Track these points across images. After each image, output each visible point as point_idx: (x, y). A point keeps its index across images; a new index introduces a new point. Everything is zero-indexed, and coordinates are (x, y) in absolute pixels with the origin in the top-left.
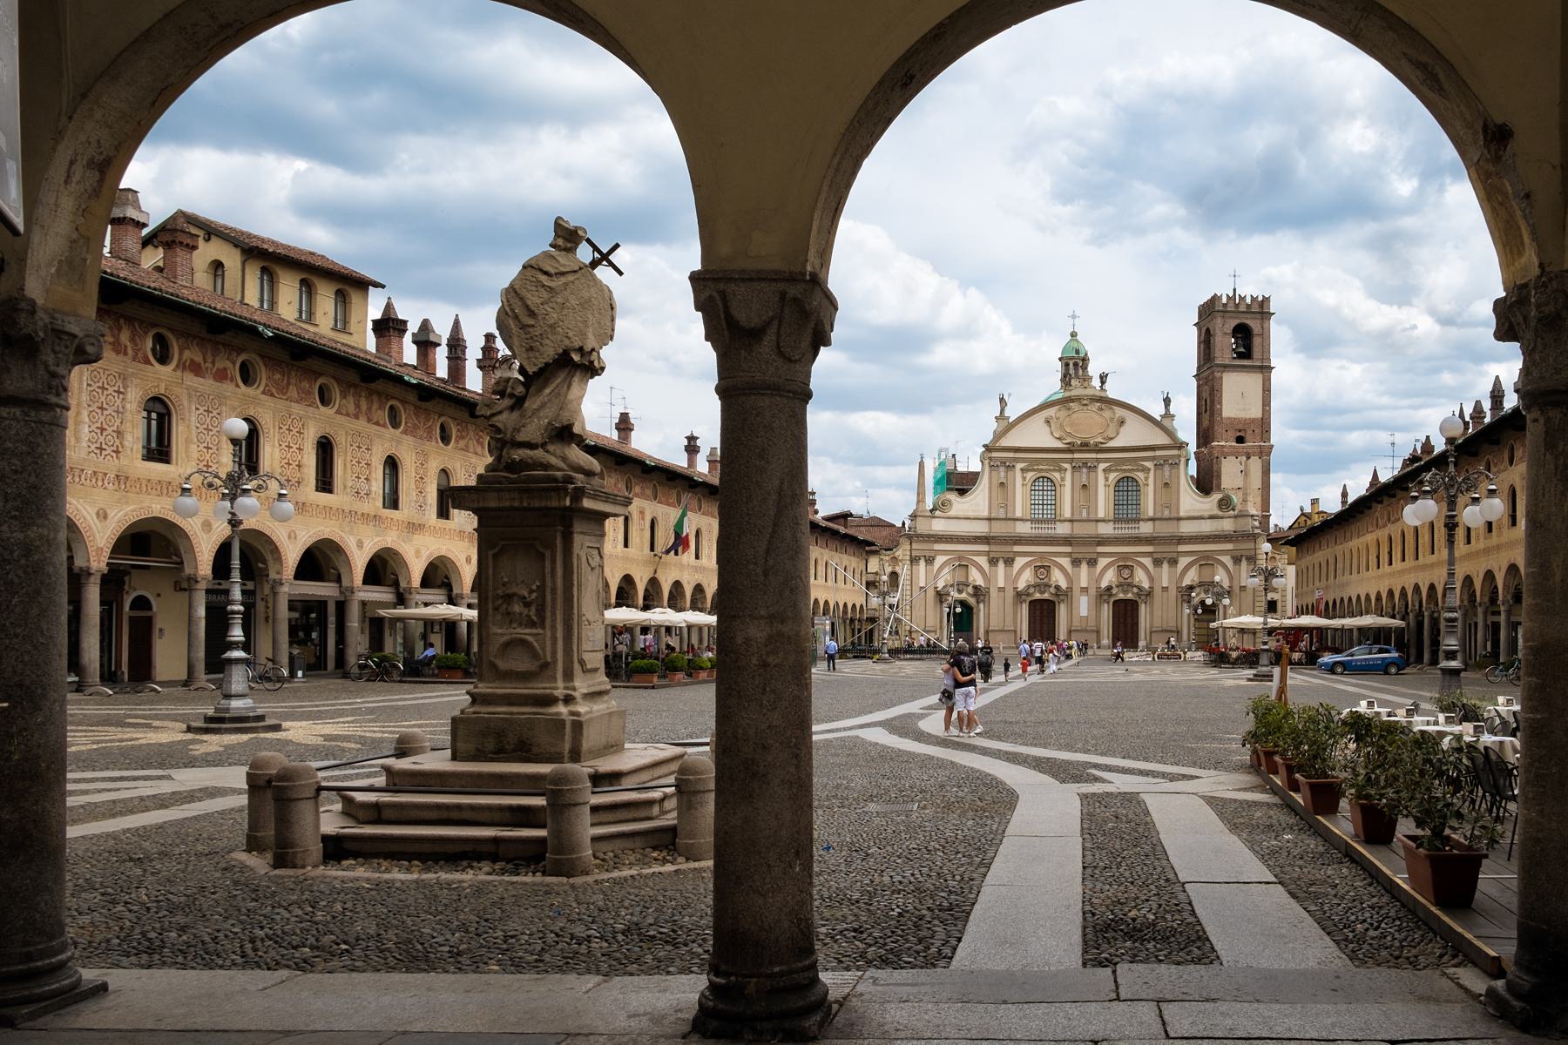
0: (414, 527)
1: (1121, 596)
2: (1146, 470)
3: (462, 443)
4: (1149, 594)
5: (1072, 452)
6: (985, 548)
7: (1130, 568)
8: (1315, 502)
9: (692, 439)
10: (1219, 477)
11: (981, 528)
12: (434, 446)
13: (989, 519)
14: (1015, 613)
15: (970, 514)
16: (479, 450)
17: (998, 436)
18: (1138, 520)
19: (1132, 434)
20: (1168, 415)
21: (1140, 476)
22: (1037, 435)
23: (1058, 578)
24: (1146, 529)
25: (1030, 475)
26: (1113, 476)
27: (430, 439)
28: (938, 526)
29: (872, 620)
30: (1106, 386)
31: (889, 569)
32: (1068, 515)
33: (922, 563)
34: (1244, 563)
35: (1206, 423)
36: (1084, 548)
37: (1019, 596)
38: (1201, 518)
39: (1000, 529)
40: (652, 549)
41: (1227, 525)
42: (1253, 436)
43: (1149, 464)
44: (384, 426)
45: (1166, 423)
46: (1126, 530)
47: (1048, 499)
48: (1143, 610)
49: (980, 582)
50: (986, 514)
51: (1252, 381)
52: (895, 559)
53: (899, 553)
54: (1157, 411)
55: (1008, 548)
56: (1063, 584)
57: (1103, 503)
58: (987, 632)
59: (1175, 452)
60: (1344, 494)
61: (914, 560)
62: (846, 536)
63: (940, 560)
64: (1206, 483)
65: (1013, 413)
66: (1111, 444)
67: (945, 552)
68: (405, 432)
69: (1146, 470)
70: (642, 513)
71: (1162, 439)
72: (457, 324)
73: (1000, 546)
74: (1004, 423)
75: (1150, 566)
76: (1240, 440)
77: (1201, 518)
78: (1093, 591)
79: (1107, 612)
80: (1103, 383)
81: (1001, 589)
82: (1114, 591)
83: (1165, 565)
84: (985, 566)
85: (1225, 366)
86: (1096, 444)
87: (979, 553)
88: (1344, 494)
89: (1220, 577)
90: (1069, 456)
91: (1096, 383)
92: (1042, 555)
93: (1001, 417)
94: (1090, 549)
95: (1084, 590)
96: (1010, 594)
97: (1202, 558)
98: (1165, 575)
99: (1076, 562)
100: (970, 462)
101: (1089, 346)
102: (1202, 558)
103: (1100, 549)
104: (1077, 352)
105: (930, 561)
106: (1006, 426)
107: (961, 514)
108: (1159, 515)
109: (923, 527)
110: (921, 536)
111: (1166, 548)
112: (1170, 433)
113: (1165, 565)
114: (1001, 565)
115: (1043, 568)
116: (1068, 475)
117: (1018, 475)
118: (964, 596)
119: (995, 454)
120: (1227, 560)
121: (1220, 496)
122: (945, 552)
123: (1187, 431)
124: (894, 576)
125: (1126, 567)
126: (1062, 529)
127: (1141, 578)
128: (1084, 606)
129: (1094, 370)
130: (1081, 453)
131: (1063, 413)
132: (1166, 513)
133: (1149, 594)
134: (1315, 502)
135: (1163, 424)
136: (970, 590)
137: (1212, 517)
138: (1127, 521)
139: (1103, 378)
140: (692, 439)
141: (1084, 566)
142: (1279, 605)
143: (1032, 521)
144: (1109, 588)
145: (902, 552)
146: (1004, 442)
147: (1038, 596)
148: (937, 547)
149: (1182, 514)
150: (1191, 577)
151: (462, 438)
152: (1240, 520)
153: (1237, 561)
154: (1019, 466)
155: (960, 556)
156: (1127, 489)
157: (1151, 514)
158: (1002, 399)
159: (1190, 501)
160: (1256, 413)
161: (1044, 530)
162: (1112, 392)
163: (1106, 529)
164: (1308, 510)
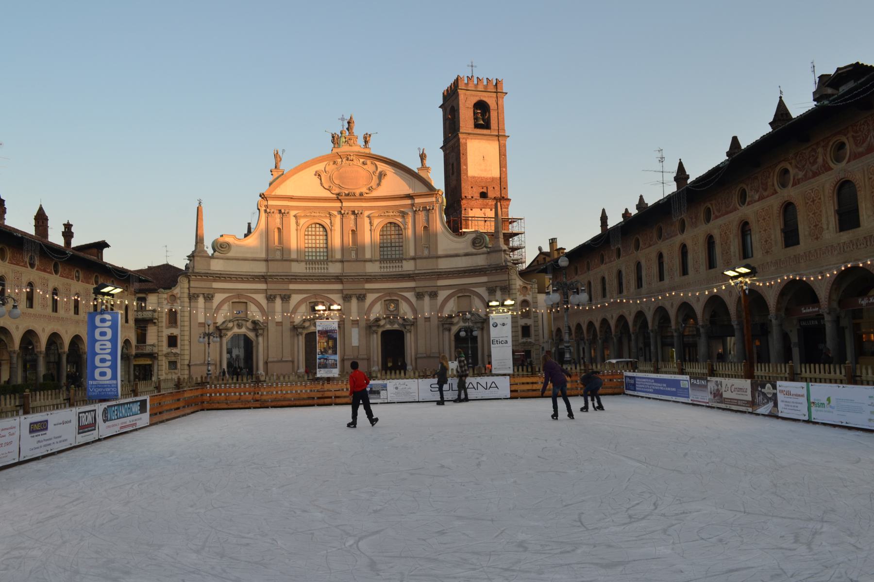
1: (388, 327)
6: (263, 286)
7: (396, 302)
8: (553, 242)
11: (260, 268)
13: (267, 260)
14: (293, 345)
18: (401, 260)
20: (424, 167)
24: (408, 267)
28: (217, 266)
30: (370, 145)
33: (201, 300)
38: (457, 256)
39: (276, 268)
41: (480, 261)
45: (422, 174)
46: (391, 269)
48: (409, 339)
49: (259, 317)
50: (263, 256)
52: (173, 298)
53: (176, 291)
54: (414, 165)
58: (266, 363)
60: (604, 219)
61: (192, 297)
63: (218, 298)
66: (374, 194)
67: (224, 291)
76: (484, 195)
77: (457, 256)
78: (363, 324)
79: (376, 340)
80: (366, 142)
82: (382, 323)
83: (427, 299)
84: (263, 302)
86: (361, 194)
87: (257, 291)
88: (604, 219)
91: (361, 142)
94: (359, 286)
95: (355, 323)
97: (460, 291)
98: (427, 308)
101: (354, 119)
102: (460, 291)
103: (368, 286)
105: (209, 298)
107: (238, 255)
109: (200, 267)
111: (428, 283)
113: (427, 299)
116: (337, 220)
117: (293, 221)
118: (243, 330)
119: (271, 203)
122: (224, 291)
125: (392, 301)
128: (355, 337)
129: (359, 131)
132: (426, 253)
133: (414, 323)
134: (553, 242)
137: (466, 255)
138: (391, 260)
141: (354, 301)
142: (532, 330)
143: (306, 262)
144: (377, 320)
146: (280, 191)
148: (216, 285)
149: (440, 252)
150: (450, 308)
152: (494, 255)
154: (293, 213)
155: (239, 294)
157: (412, 253)
158: (276, 155)
160: (496, 174)
161: (318, 270)
164: (546, 249)
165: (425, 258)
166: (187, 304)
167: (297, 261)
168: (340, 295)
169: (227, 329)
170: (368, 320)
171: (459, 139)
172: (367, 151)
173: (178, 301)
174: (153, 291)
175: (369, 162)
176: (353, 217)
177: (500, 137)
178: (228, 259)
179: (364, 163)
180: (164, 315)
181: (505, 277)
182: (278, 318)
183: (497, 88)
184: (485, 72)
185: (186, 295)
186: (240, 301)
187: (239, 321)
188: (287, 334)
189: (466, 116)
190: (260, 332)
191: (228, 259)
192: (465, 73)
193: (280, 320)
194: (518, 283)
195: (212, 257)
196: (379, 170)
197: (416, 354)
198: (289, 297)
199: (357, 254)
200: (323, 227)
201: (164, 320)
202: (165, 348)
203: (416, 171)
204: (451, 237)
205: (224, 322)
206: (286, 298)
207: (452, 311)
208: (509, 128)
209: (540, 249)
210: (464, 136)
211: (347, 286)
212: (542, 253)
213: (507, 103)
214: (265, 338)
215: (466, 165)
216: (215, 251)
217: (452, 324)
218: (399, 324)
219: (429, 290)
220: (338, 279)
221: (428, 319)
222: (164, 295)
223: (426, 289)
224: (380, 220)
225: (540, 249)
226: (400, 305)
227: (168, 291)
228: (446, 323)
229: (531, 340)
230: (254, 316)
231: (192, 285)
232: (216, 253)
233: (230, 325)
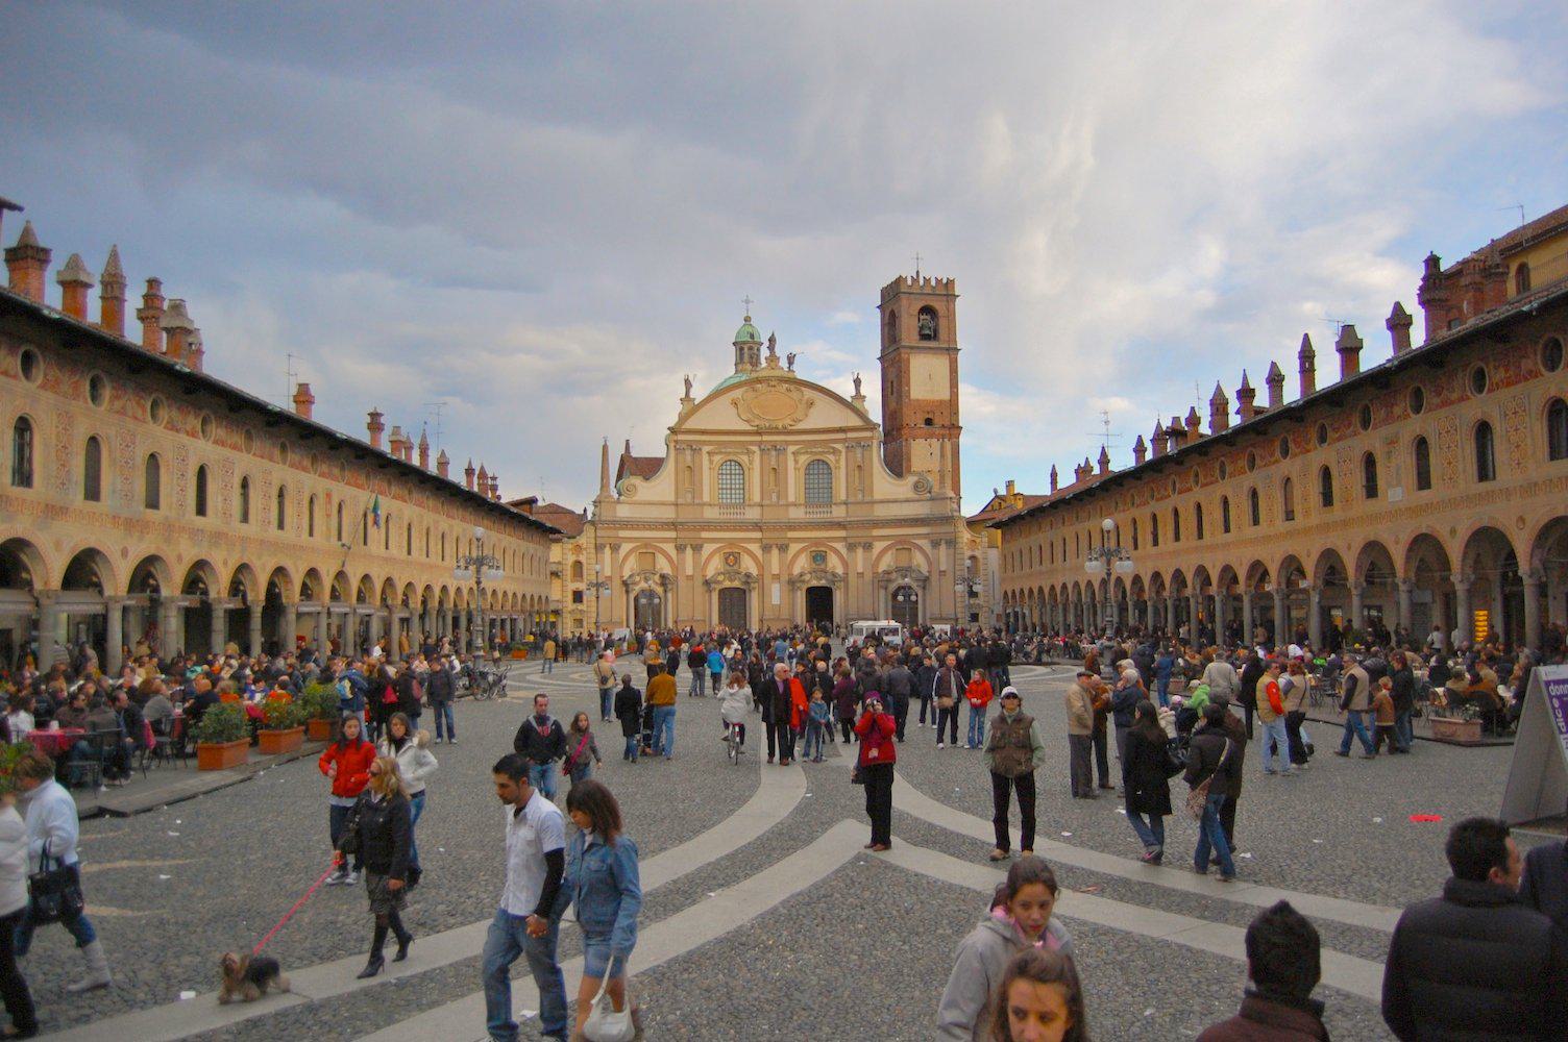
0: (54, 511)
2: (835, 452)
3: (118, 404)
4: (845, 579)
5: (758, 433)
6: (673, 534)
8: (1010, 484)
9: (375, 416)
10: (909, 460)
11: (669, 514)
12: (81, 406)
15: (656, 499)
16: (139, 414)
17: (683, 418)
18: (830, 504)
19: (824, 416)
20: (859, 396)
21: (830, 459)
22: (724, 417)
23: (748, 565)
24: (839, 513)
25: (717, 458)
26: (804, 459)
27: (76, 397)
28: (623, 512)
29: (556, 612)
30: (794, 367)
31: (571, 559)
32: (757, 498)
33: (607, 551)
34: (943, 547)
35: (893, 405)
36: (775, 536)
37: (707, 583)
38: (895, 501)
39: (687, 515)
40: (340, 539)
42: (943, 422)
43: (838, 446)
44: (15, 377)
45: (857, 404)
46: (819, 515)
47: (737, 480)
48: (838, 598)
49: (667, 570)
50: (672, 498)
51: (940, 364)
52: (578, 548)
53: (582, 540)
54: (847, 390)
55: (696, 535)
56: (754, 571)
57: (794, 487)
59: (868, 434)
60: (1054, 476)
61: (599, 548)
62: (535, 522)
63: (625, 548)
64: (897, 465)
65: (699, 393)
66: (801, 426)
67: (630, 540)
68: (43, 387)
69: (835, 452)
70: (329, 496)
71: (856, 421)
72: (114, 257)
73: (687, 531)
74: (689, 406)
75: (844, 551)
78: (785, 578)
79: (801, 599)
81: (690, 578)
82: (807, 577)
83: (860, 551)
84: (673, 553)
85: (912, 348)
88: (1054, 476)
89: (918, 560)
90: (758, 438)
91: (784, 363)
92: (731, 542)
93: (687, 398)
95: (777, 577)
96: (699, 581)
97: (900, 542)
99: (766, 549)
100: (651, 445)
103: (791, 534)
104: (752, 336)
105: (615, 548)
106: (691, 408)
108: (851, 500)
109: (606, 515)
110: (606, 522)
112: (862, 415)
113: (860, 551)
114: (775, 552)
115: (732, 559)
116: (757, 458)
119: (680, 437)
120: (925, 544)
121: (915, 479)
122: (630, 540)
123: (876, 415)
124: (578, 564)
126: (752, 514)
127: (834, 564)
128: (776, 594)
129: (781, 351)
130: (769, 437)
131: (751, 394)
134: (1010, 484)
135: (854, 406)
136: (657, 578)
137: (907, 501)
139: (791, 359)
140: (375, 416)
143: (720, 506)
145: (586, 539)
146: (690, 424)
147: (727, 584)
148: (622, 534)
149: (877, 496)
150: (886, 563)
151: (118, 397)
153: (935, 544)
154: (706, 449)
155: (647, 543)
156: (818, 470)
157: (843, 497)
159: (884, 484)
160: (945, 395)
162: (800, 373)
163: (797, 514)
164: (1002, 491)
165: (859, 503)
166: (594, 556)
167: (710, 505)
168: (758, 545)
169: (635, 584)
170: (790, 574)
171: (900, 354)
172: (790, 375)
173: (584, 552)
174: (557, 541)
175: (792, 387)
176: (774, 453)
177: (952, 351)
178: (635, 503)
179: (789, 390)
180: (569, 568)
181: (950, 529)
182: (689, 571)
183: (947, 290)
184: (934, 271)
185: (593, 546)
186: (648, 551)
187: (646, 575)
188: (700, 589)
189: (909, 325)
190: (670, 587)
191: (635, 503)
192: (908, 273)
193: (690, 573)
194: (966, 535)
195: (618, 502)
196: (806, 397)
197: (846, 615)
198: (701, 546)
199: (778, 498)
200: (740, 465)
201: (569, 572)
202: (570, 605)
203: (850, 400)
204: (889, 479)
205: (630, 576)
206: (697, 548)
207: (889, 566)
208: (961, 342)
209: (995, 491)
210: (906, 350)
211: (768, 534)
212: (997, 497)
213: (960, 305)
214: (675, 595)
215: (908, 384)
216: (620, 494)
217: (889, 581)
218: (827, 580)
219: (863, 540)
220: (757, 526)
221: (861, 575)
222: (569, 545)
223: (858, 540)
224: (806, 457)
225: (995, 491)
226: (828, 557)
227: (572, 541)
228: (883, 580)
229: (980, 601)
230: (662, 569)
231: (598, 534)
232: (622, 498)
233: (638, 578)
